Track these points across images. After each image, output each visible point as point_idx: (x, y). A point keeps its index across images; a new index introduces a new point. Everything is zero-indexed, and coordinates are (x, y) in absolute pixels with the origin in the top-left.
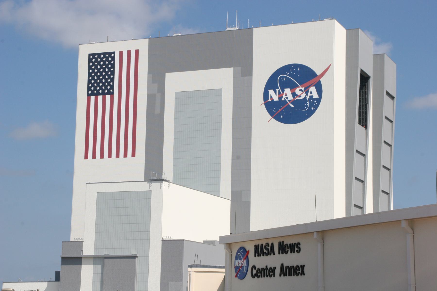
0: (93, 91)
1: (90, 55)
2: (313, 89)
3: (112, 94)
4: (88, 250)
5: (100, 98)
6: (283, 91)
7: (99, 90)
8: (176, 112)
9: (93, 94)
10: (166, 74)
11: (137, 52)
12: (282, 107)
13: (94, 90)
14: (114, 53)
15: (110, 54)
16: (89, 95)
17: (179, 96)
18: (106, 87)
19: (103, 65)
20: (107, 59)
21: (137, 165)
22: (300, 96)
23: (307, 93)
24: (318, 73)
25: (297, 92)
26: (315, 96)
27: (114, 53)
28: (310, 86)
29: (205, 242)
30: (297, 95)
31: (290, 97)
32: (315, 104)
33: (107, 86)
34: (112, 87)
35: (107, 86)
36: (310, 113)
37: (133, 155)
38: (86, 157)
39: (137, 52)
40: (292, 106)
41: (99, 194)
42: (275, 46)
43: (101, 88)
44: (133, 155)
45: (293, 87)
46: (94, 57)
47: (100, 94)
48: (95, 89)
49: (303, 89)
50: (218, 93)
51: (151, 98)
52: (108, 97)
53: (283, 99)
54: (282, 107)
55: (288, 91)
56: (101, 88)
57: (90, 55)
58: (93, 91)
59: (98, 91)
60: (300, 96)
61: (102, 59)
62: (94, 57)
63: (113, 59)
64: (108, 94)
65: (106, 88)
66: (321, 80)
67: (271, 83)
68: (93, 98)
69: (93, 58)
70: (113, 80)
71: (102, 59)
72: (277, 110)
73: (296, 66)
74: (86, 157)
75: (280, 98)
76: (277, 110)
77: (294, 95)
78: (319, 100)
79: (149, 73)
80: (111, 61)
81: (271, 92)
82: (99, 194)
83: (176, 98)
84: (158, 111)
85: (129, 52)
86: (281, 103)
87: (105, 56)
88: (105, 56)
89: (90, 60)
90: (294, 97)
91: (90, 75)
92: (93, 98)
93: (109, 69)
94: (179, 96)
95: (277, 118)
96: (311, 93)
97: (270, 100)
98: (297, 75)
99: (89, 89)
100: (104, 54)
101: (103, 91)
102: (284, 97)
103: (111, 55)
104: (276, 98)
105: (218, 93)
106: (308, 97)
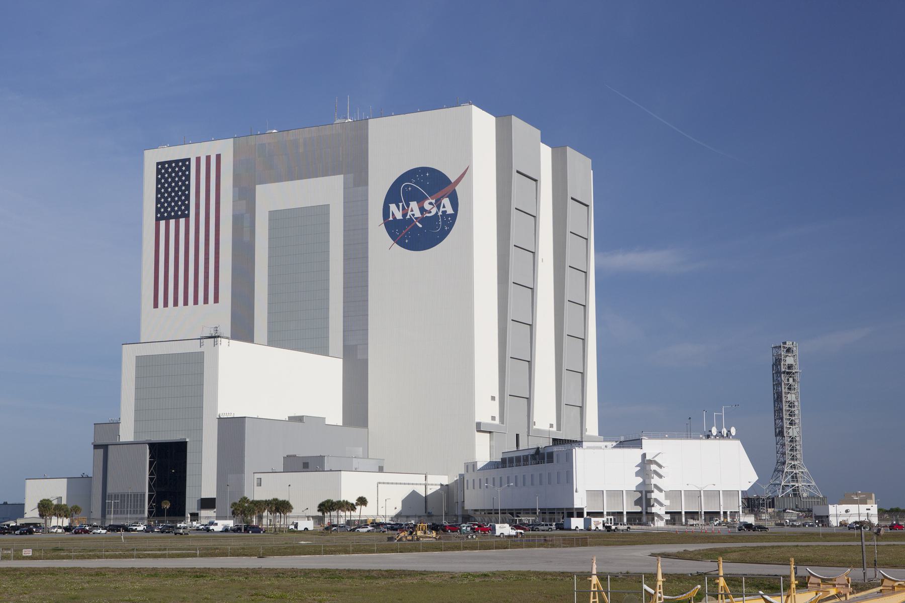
0: (162, 214)
1: (158, 164)
2: (446, 201)
3: (187, 217)
4: (127, 434)
5: (172, 222)
6: (408, 207)
7: (170, 212)
9: (163, 218)
10: (257, 186)
11: (218, 157)
12: (408, 228)
13: (164, 213)
14: (189, 160)
15: (184, 161)
16: (158, 220)
17: (274, 216)
18: (179, 207)
19: (175, 177)
20: (180, 168)
21: (220, 314)
22: (430, 212)
23: (438, 207)
24: (453, 180)
25: (427, 206)
26: (450, 210)
27: (189, 160)
28: (443, 197)
29: (291, 419)
30: (426, 211)
31: (418, 214)
32: (449, 221)
33: (181, 205)
34: (188, 207)
35: (181, 205)
36: (443, 235)
37: (216, 300)
38: (156, 305)
39: (218, 157)
40: (420, 226)
41: (138, 358)
42: (397, 143)
43: (173, 210)
44: (216, 300)
45: (420, 199)
46: (163, 167)
47: (172, 218)
48: (166, 211)
49: (433, 201)
50: (323, 211)
51: (237, 220)
52: (182, 221)
53: (408, 217)
54: (408, 228)
55: (414, 205)
56: (173, 210)
57: (158, 164)
60: (430, 212)
61: (173, 169)
62: (163, 167)
63: (188, 168)
64: (181, 216)
65: (180, 209)
66: (457, 188)
67: (393, 196)
69: (162, 167)
70: (188, 197)
71: (173, 169)
72: (400, 232)
74: (156, 305)
75: (404, 215)
76: (400, 232)
77: (422, 210)
78: (454, 217)
79: (234, 186)
80: (185, 171)
81: (393, 207)
82: (138, 358)
83: (270, 220)
85: (208, 158)
86: (406, 222)
87: (177, 165)
88: (177, 165)
89: (158, 171)
90: (422, 213)
91: (158, 191)
92: (163, 223)
93: (183, 182)
94: (274, 216)
96: (444, 207)
97: (391, 218)
98: (425, 183)
99: (158, 210)
100: (177, 162)
101: (176, 212)
102: (410, 213)
103: (186, 162)
104: (399, 216)
105: (323, 211)
106: (440, 213)
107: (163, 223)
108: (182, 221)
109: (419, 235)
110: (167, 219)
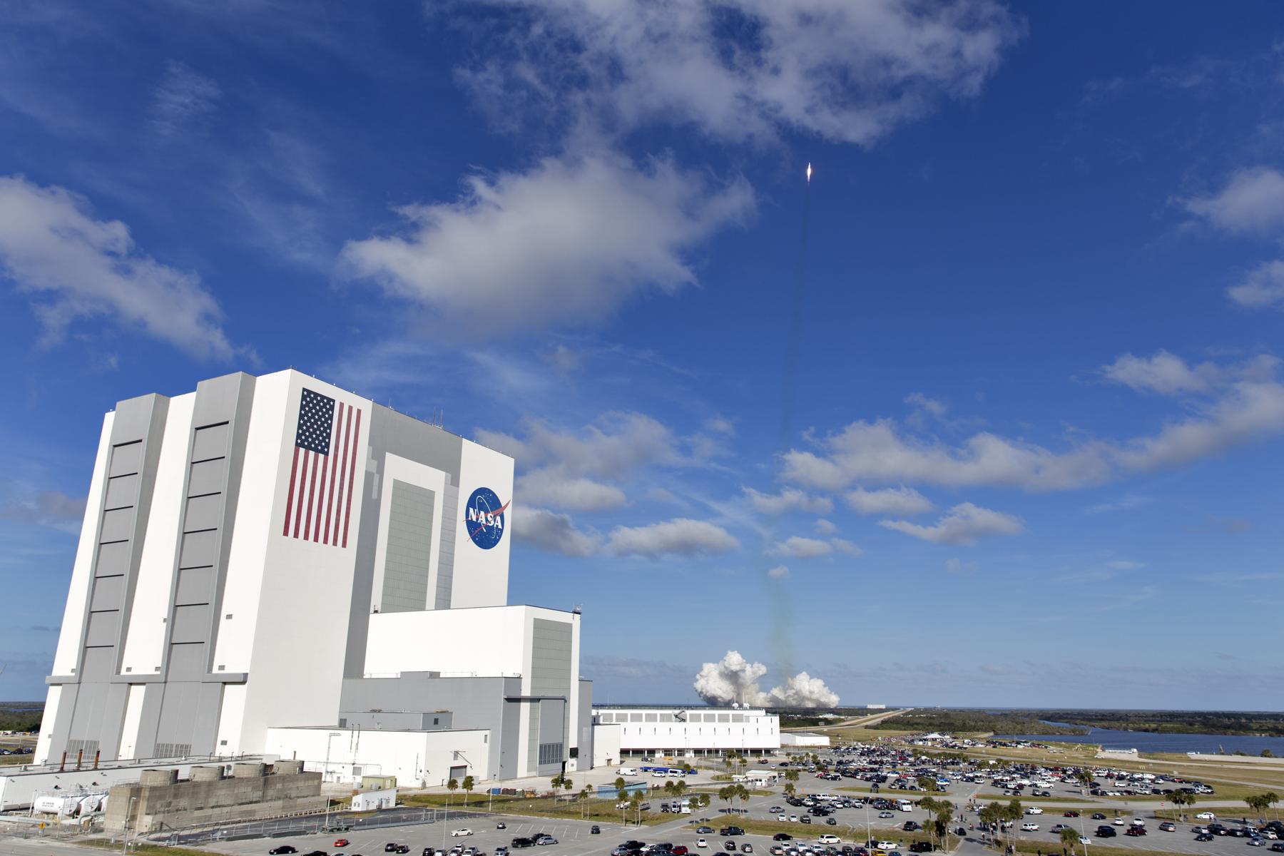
1: (304, 390)
2: (498, 518)
3: (327, 454)
8: (393, 503)
10: (388, 454)
11: (359, 411)
15: (330, 400)
17: (398, 485)
20: (325, 406)
34: (328, 445)
36: (496, 541)
37: (344, 545)
38: (286, 533)
39: (359, 411)
44: (344, 545)
45: (487, 512)
48: (306, 440)
50: (431, 495)
51: (369, 477)
55: (482, 513)
57: (304, 390)
58: (303, 441)
59: (310, 444)
61: (318, 402)
63: (332, 408)
67: (471, 503)
68: (302, 451)
71: (318, 402)
73: (490, 492)
74: (286, 533)
84: (375, 496)
85: (350, 408)
89: (304, 398)
94: (398, 485)
95: (474, 539)
99: (299, 436)
100: (323, 397)
107: (302, 451)
108: (321, 456)
109: (485, 538)
110: (308, 448)
